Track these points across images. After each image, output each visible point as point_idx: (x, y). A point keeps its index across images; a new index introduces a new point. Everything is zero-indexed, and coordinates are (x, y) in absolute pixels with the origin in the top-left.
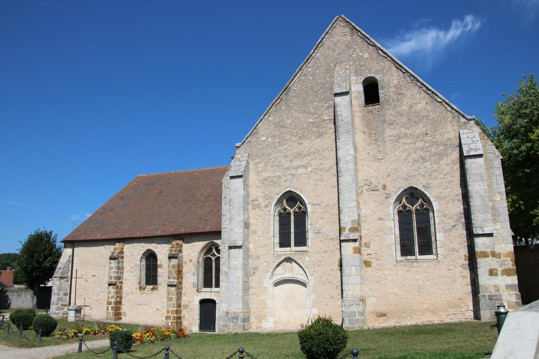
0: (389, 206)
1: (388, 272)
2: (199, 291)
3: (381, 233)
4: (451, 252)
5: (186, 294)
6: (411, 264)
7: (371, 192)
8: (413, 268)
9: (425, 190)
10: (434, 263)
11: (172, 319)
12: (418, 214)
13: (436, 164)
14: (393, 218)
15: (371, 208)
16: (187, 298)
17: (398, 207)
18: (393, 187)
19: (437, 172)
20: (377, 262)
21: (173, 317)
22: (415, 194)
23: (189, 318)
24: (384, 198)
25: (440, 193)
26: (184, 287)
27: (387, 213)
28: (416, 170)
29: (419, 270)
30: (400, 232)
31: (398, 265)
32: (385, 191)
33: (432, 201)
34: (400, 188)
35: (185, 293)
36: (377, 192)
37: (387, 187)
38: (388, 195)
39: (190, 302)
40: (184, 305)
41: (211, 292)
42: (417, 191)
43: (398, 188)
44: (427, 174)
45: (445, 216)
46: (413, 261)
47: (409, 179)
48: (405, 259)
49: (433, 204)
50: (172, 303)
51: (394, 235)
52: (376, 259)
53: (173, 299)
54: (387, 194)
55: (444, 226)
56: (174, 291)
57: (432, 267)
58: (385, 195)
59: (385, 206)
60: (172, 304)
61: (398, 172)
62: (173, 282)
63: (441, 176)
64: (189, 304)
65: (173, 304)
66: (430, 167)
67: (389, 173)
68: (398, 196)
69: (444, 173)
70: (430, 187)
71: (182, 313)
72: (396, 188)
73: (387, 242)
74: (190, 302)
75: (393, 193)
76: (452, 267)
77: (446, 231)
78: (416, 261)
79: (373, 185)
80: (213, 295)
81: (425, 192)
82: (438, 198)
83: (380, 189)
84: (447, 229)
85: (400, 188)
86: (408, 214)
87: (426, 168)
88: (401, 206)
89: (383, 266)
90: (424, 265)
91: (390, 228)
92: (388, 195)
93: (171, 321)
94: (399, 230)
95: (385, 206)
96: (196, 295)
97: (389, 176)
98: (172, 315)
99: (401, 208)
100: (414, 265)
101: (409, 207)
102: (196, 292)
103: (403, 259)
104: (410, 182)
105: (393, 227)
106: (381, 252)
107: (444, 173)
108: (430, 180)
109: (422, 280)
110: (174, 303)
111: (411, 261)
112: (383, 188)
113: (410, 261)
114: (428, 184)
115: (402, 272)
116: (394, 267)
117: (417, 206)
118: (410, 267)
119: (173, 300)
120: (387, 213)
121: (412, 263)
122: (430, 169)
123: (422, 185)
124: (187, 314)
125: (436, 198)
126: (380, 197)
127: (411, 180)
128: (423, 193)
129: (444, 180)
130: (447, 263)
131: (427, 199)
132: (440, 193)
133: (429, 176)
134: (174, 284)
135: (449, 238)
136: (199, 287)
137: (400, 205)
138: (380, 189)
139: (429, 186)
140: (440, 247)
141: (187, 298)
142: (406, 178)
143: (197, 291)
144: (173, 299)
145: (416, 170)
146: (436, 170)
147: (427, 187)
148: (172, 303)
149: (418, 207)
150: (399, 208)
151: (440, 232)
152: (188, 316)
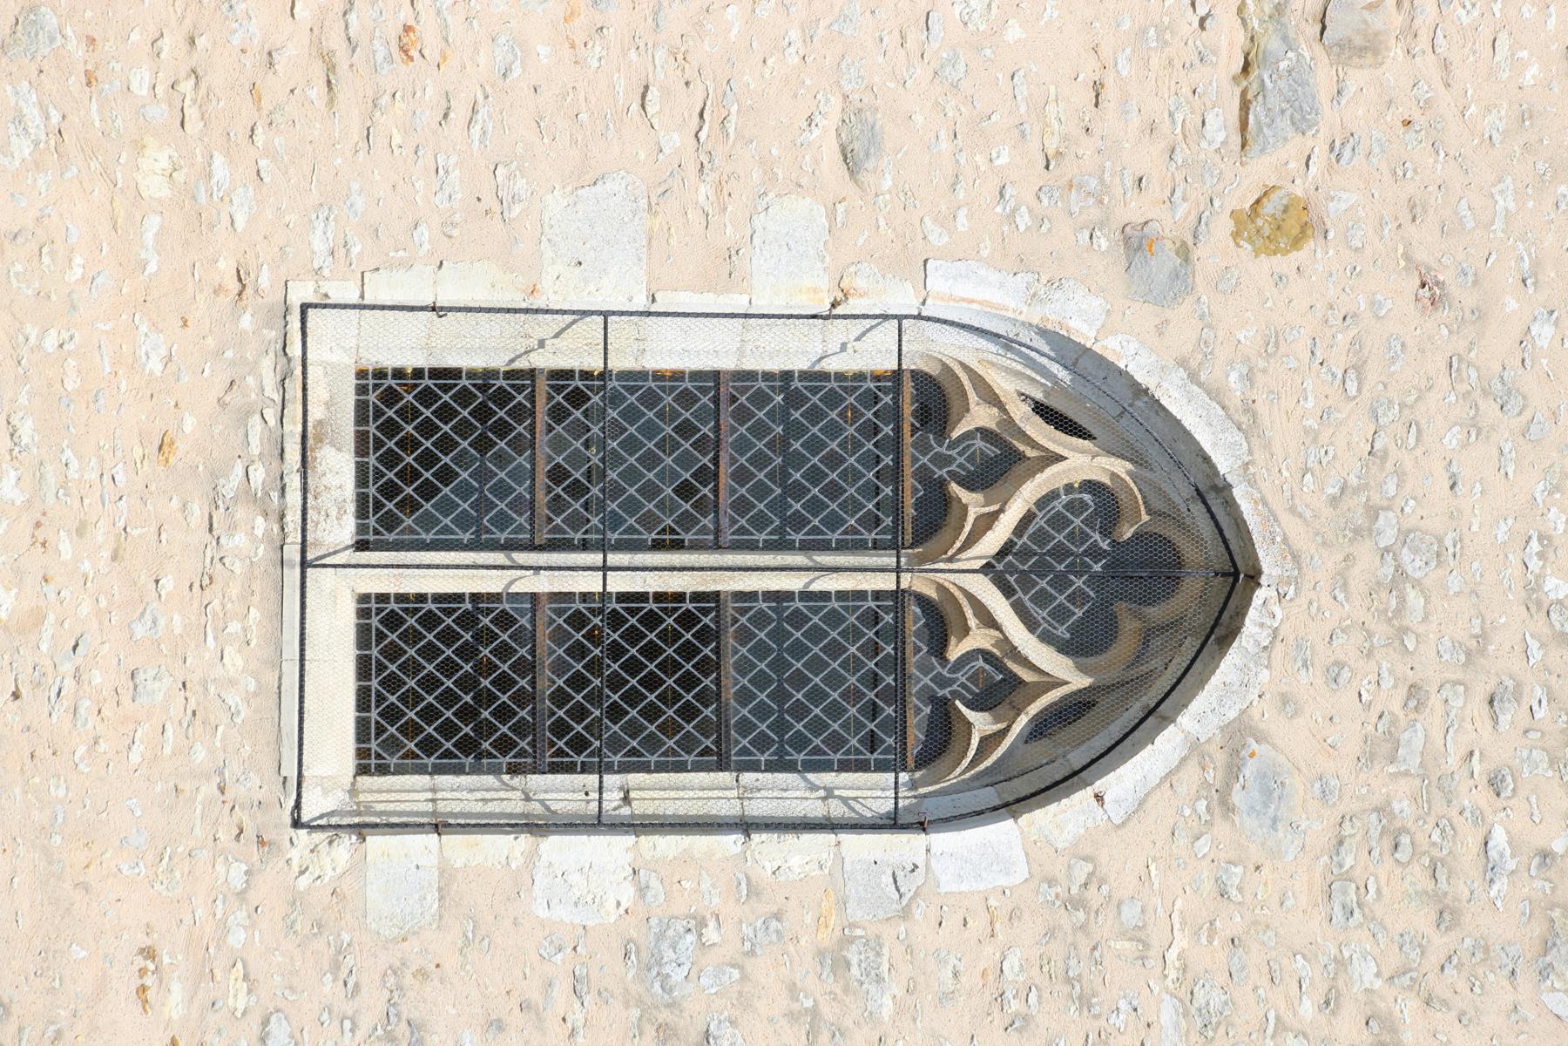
0: (1021, 265)
1: (155, 187)
3: (676, 141)
4: (373, 1002)
6: (247, 494)
7: (1228, 40)
8: (198, 512)
9: (1195, 748)
10: (255, 784)
12: (897, 634)
13: (1537, 929)
14: (853, 306)
15: (1014, 32)
17: (1005, 386)
18: (1272, 343)
19: (1422, 920)
20: (294, 52)
22: (1157, 613)
24: (1135, 209)
25: (1137, 935)
27: (938, 238)
28: (1475, 651)
29: (167, 584)
30: (677, 376)
31: (246, 322)
32: (1223, 227)
33: (1045, 819)
34: (1247, 422)
36: (1221, 124)
37: (1284, 264)
38: (1167, 258)
42: (1191, 644)
43: (1249, 407)
44: (1404, 786)
45: (840, 965)
46: (293, 518)
47: (1365, 554)
48: (315, 413)
49: (1002, 832)
51: (641, 303)
52: (336, 42)
54: (1184, 253)
55: (711, 934)
57: (200, 754)
58: (1171, 222)
59: (1024, 220)
61: (1475, 428)
63: (1365, 974)
66: (1499, 838)
67: (1464, 296)
68: (1140, 391)
69: (1408, 1009)
70: (1228, 809)
72: (1249, 377)
73: (555, 203)
75: (1183, 336)
76: (174, 1003)
77: (652, 966)
78: (292, 552)
79: (1323, 78)
81: (1163, 750)
82: (1073, 903)
83: (1260, 170)
84: (677, 976)
85: (1247, 422)
86: (896, 509)
87: (1495, 784)
88: (1009, 422)
89: (241, 133)
90: (235, 660)
91: (732, 253)
92: (1167, 258)
94: (697, 375)
95: (1024, 220)
97: (1431, 291)
99: (980, 416)
100: (232, 528)
101: (988, 521)
103: (317, 393)
104: (1322, 565)
105: (738, 303)
106: (429, 116)
107: (1408, 1009)
108: (1318, 828)
109: (38, 618)
111: (293, 497)
112: (1269, 208)
113: (294, 482)
114: (1272, 788)
115: (155, 366)
116: (226, 266)
117: (989, 621)
118: (215, 475)
120: (938, 238)
121: (258, 502)
122: (1472, 841)
123: (1267, 716)
125: (1082, 871)
126: (1148, 159)
127: (1341, 581)
128: (1156, 715)
129: (1308, 1009)
130: (237, 938)
131: (1077, 758)
132: (1137, 935)
133: (1383, 810)
135: (562, 989)
137: (1021, 413)
138: (1260, 170)
139: (1237, 797)
140: (446, 875)
142: (1373, 513)
145: (1475, 651)
146: (1446, 916)
147: (1233, 771)
149: (979, 639)
150: (992, 398)
151: (642, 891)
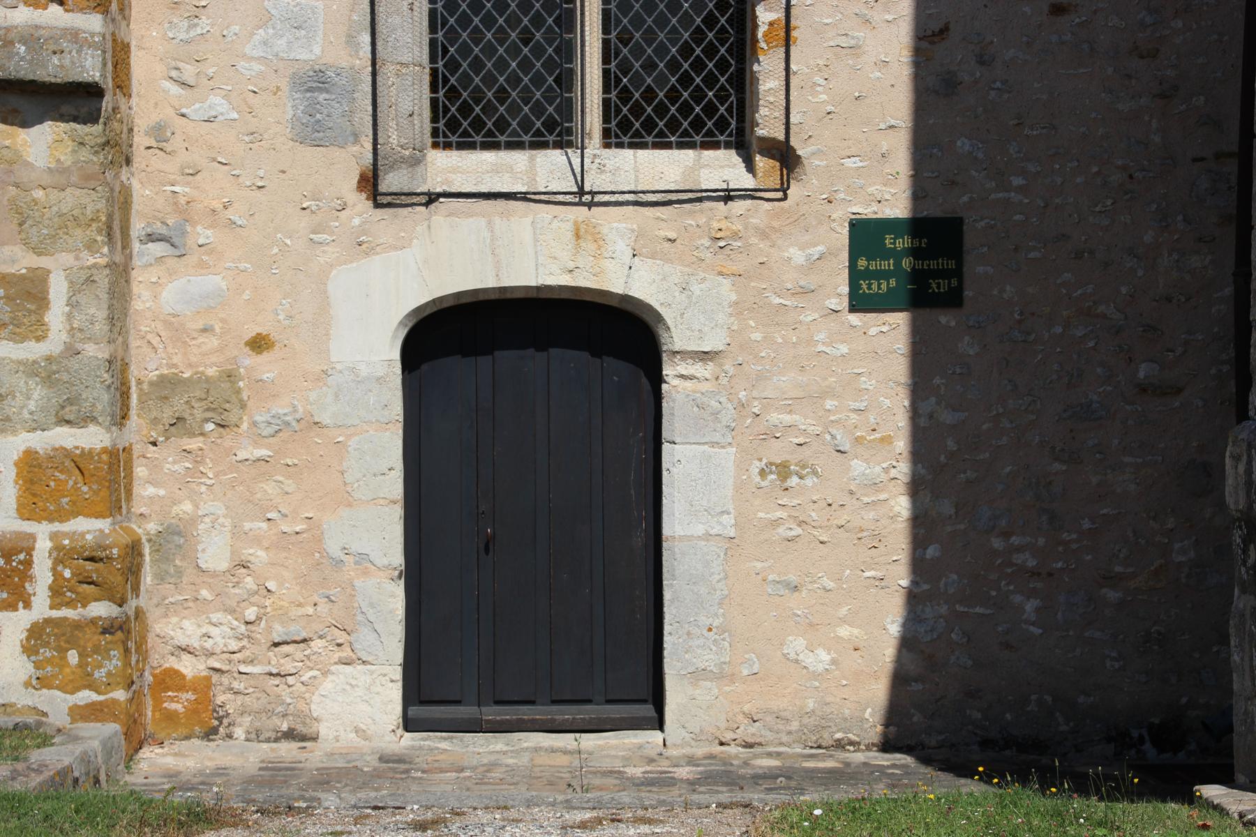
2: (391, 181)
5: (203, 234)
11: (57, 592)
16: (214, 282)
21: (61, 556)
23: (259, 556)
26: (160, 133)
35: (185, 211)
39: (259, 344)
40: (167, 385)
41: (583, 196)
50: (33, 350)
53: (42, 301)
56: (60, 177)
60: (30, 369)
62: (31, 37)
64: (249, 360)
65: (46, 372)
71: (146, 491)
74: (259, 344)
80: (622, 248)
93: (41, 607)
96: (361, 246)
98: (43, 536)
102: (360, 203)
110: (72, 351)
119: (56, 316)
124: (218, 508)
134: (54, 70)
136: (392, 137)
141: (214, 282)
143: (370, 183)
144: (58, 289)
148: (33, 350)
152: (238, 533)
